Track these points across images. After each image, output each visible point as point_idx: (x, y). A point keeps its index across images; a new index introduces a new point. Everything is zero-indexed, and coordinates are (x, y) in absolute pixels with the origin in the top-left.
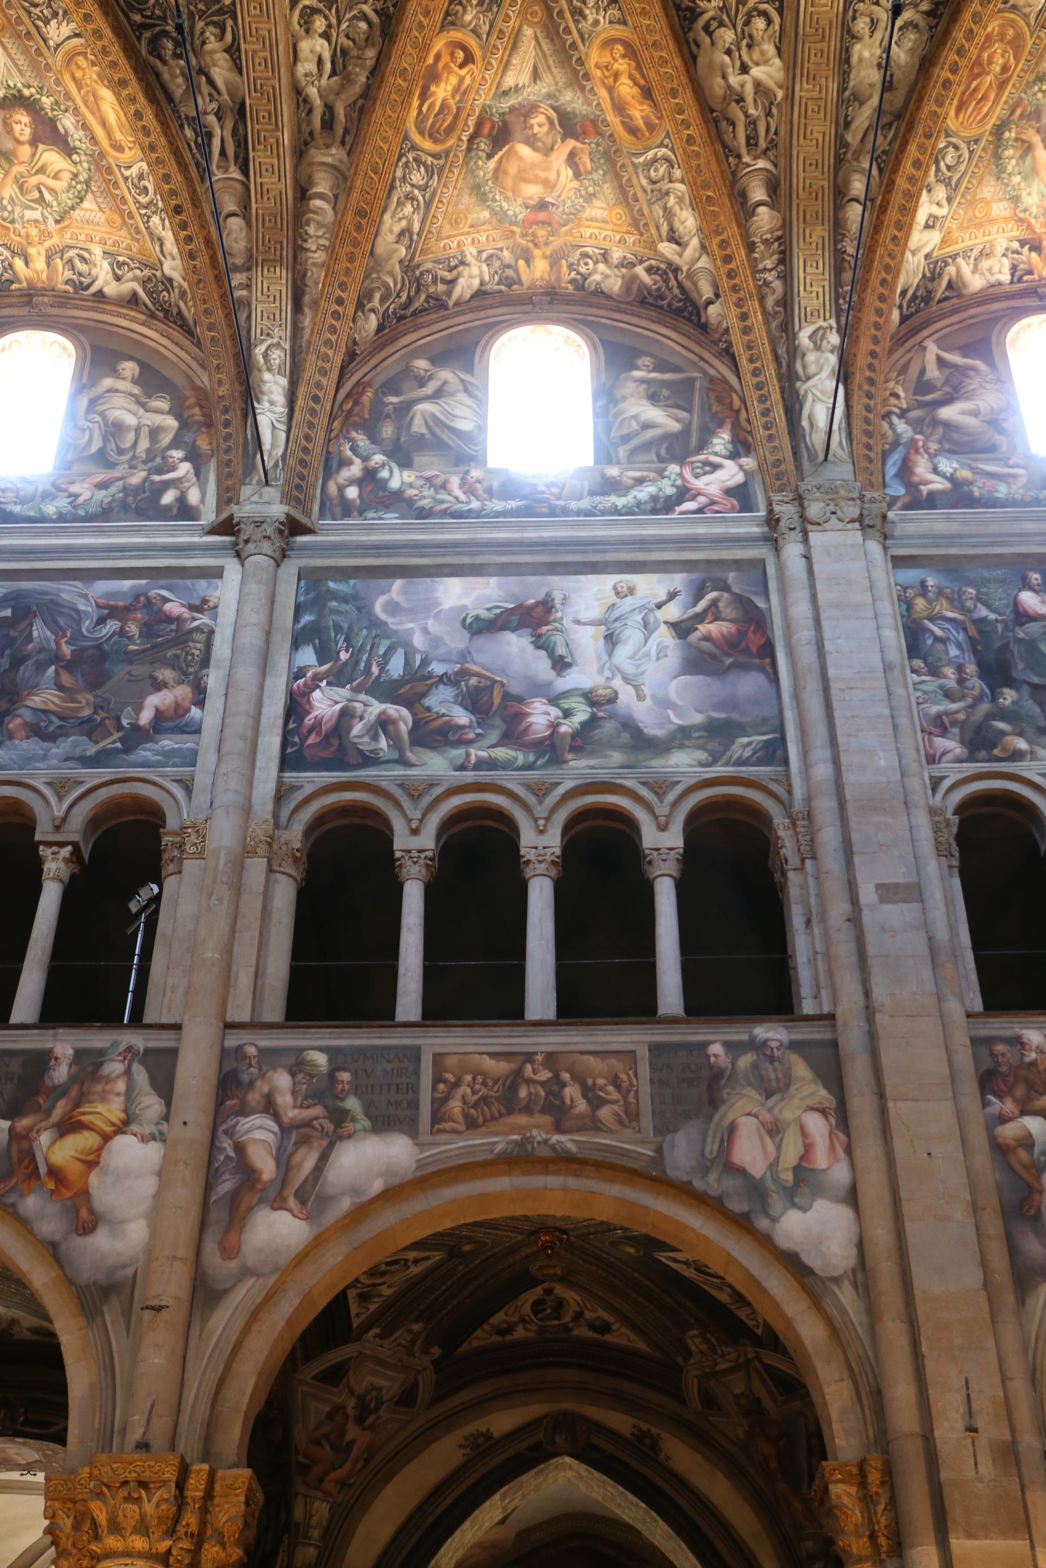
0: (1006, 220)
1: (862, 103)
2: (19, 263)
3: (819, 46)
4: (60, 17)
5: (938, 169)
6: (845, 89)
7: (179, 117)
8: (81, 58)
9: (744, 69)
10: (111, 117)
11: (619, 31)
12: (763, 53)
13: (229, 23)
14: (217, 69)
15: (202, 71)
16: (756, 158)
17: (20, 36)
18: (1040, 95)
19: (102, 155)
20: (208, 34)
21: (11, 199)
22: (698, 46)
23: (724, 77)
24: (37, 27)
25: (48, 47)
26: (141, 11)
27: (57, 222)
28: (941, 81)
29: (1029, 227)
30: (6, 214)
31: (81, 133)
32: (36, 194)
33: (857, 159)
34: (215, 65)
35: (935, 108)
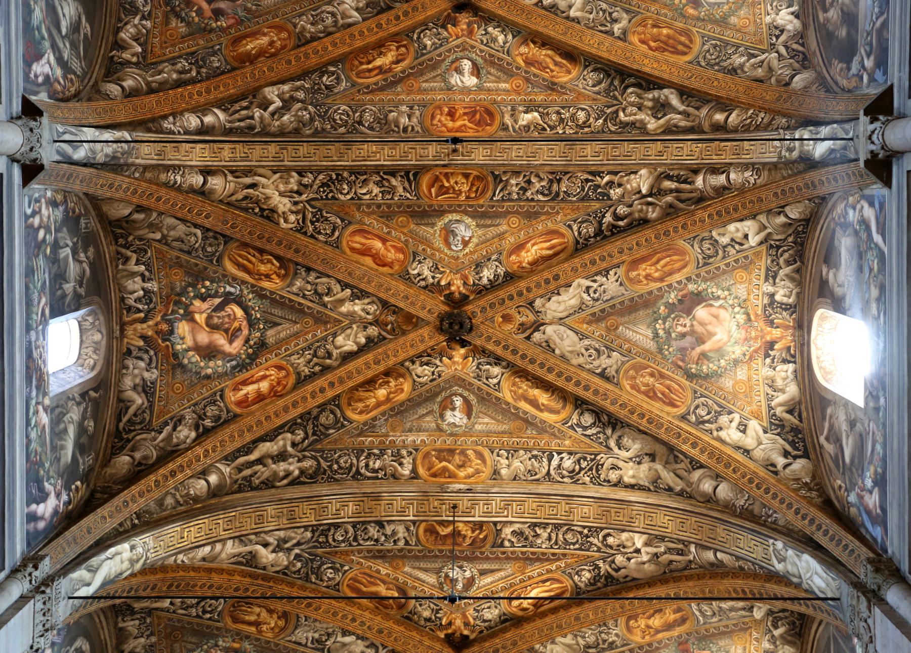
0: (749, 369)
1: (659, 478)
3: (613, 515)
5: (708, 422)
6: (649, 490)
9: (638, 551)
11: (622, 621)
12: (627, 540)
16: (690, 552)
18: (671, 350)
22: (627, 576)
23: (644, 563)
28: (648, 425)
29: (756, 351)
33: (692, 484)
35: (663, 430)
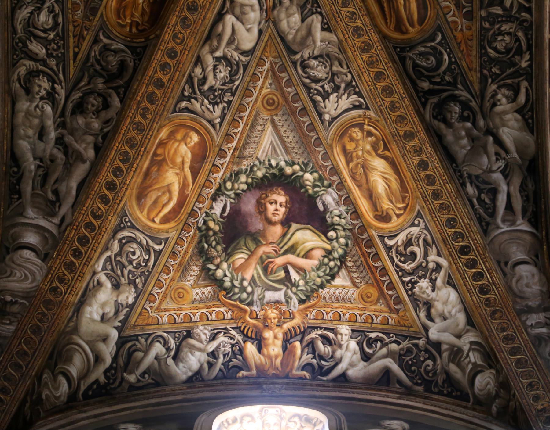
2: (251, 348)
4: (341, 91)
7: (461, 176)
8: (357, 130)
10: (380, 187)
13: (524, 84)
14: (506, 130)
15: (489, 132)
17: (293, 113)
19: (363, 229)
20: (499, 96)
21: (253, 279)
24: (314, 102)
25: (322, 122)
26: (429, 79)
27: (301, 302)
30: (245, 295)
31: (343, 208)
32: (282, 274)
34: (504, 126)
